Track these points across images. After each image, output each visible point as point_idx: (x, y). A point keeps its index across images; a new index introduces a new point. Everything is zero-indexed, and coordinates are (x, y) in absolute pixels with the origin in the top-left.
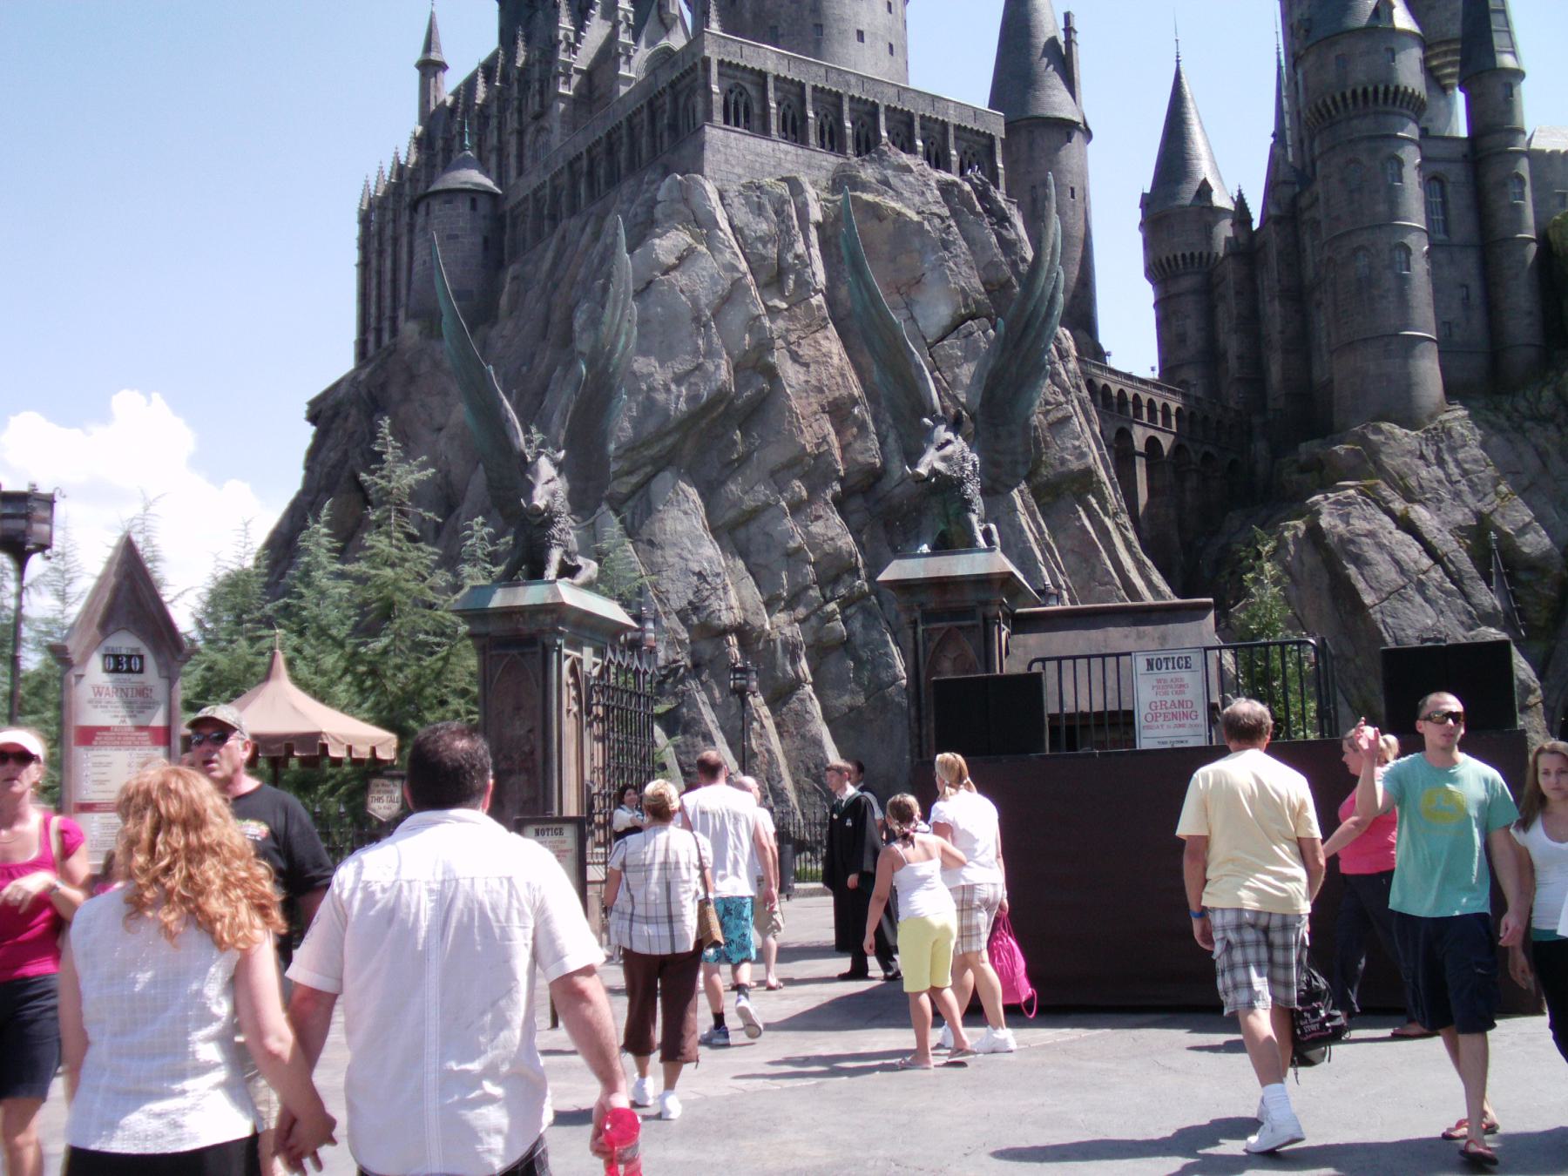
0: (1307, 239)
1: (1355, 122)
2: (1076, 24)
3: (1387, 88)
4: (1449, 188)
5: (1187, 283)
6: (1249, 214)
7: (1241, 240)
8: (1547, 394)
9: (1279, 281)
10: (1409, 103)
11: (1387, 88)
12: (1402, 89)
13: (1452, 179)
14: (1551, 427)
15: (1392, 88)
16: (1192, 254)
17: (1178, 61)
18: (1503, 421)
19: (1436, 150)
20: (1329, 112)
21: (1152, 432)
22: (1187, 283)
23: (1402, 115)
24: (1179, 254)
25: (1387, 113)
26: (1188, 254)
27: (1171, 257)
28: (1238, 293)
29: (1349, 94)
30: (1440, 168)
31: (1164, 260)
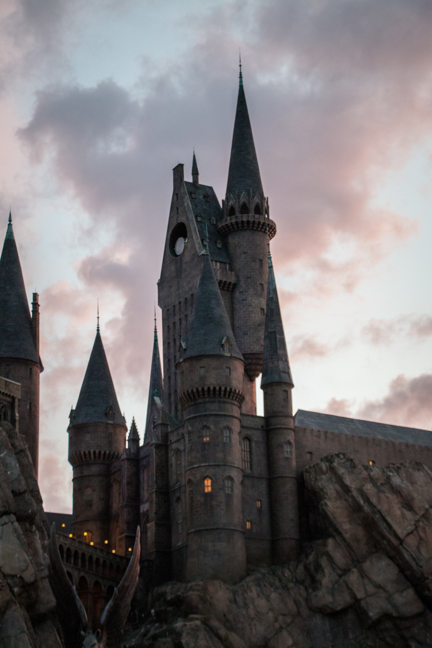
0: (173, 460)
1: (208, 405)
2: (40, 301)
3: (226, 389)
4: (253, 444)
5: (95, 469)
6: (138, 436)
7: (132, 451)
8: (301, 567)
9: (156, 482)
10: (236, 398)
11: (226, 389)
12: (233, 390)
13: (255, 439)
14: (302, 587)
15: (228, 389)
16: (100, 452)
17: (98, 330)
18: (277, 583)
19: (248, 422)
20: (194, 396)
21: (82, 574)
22: (95, 469)
23: (232, 404)
24: (92, 451)
25: (225, 402)
26: (97, 451)
27: (87, 452)
28: (128, 483)
29: (206, 389)
30: (249, 432)
31: (82, 453)
